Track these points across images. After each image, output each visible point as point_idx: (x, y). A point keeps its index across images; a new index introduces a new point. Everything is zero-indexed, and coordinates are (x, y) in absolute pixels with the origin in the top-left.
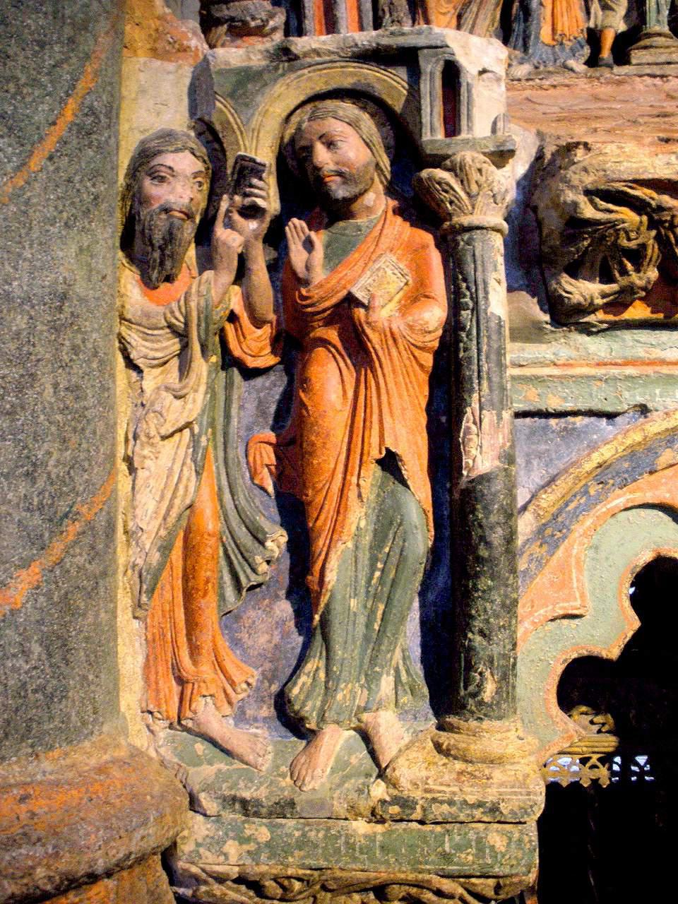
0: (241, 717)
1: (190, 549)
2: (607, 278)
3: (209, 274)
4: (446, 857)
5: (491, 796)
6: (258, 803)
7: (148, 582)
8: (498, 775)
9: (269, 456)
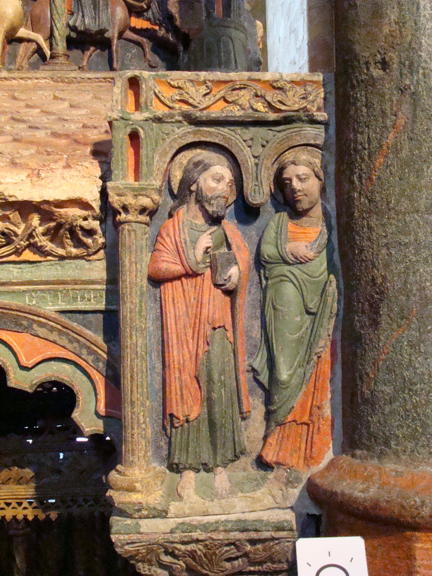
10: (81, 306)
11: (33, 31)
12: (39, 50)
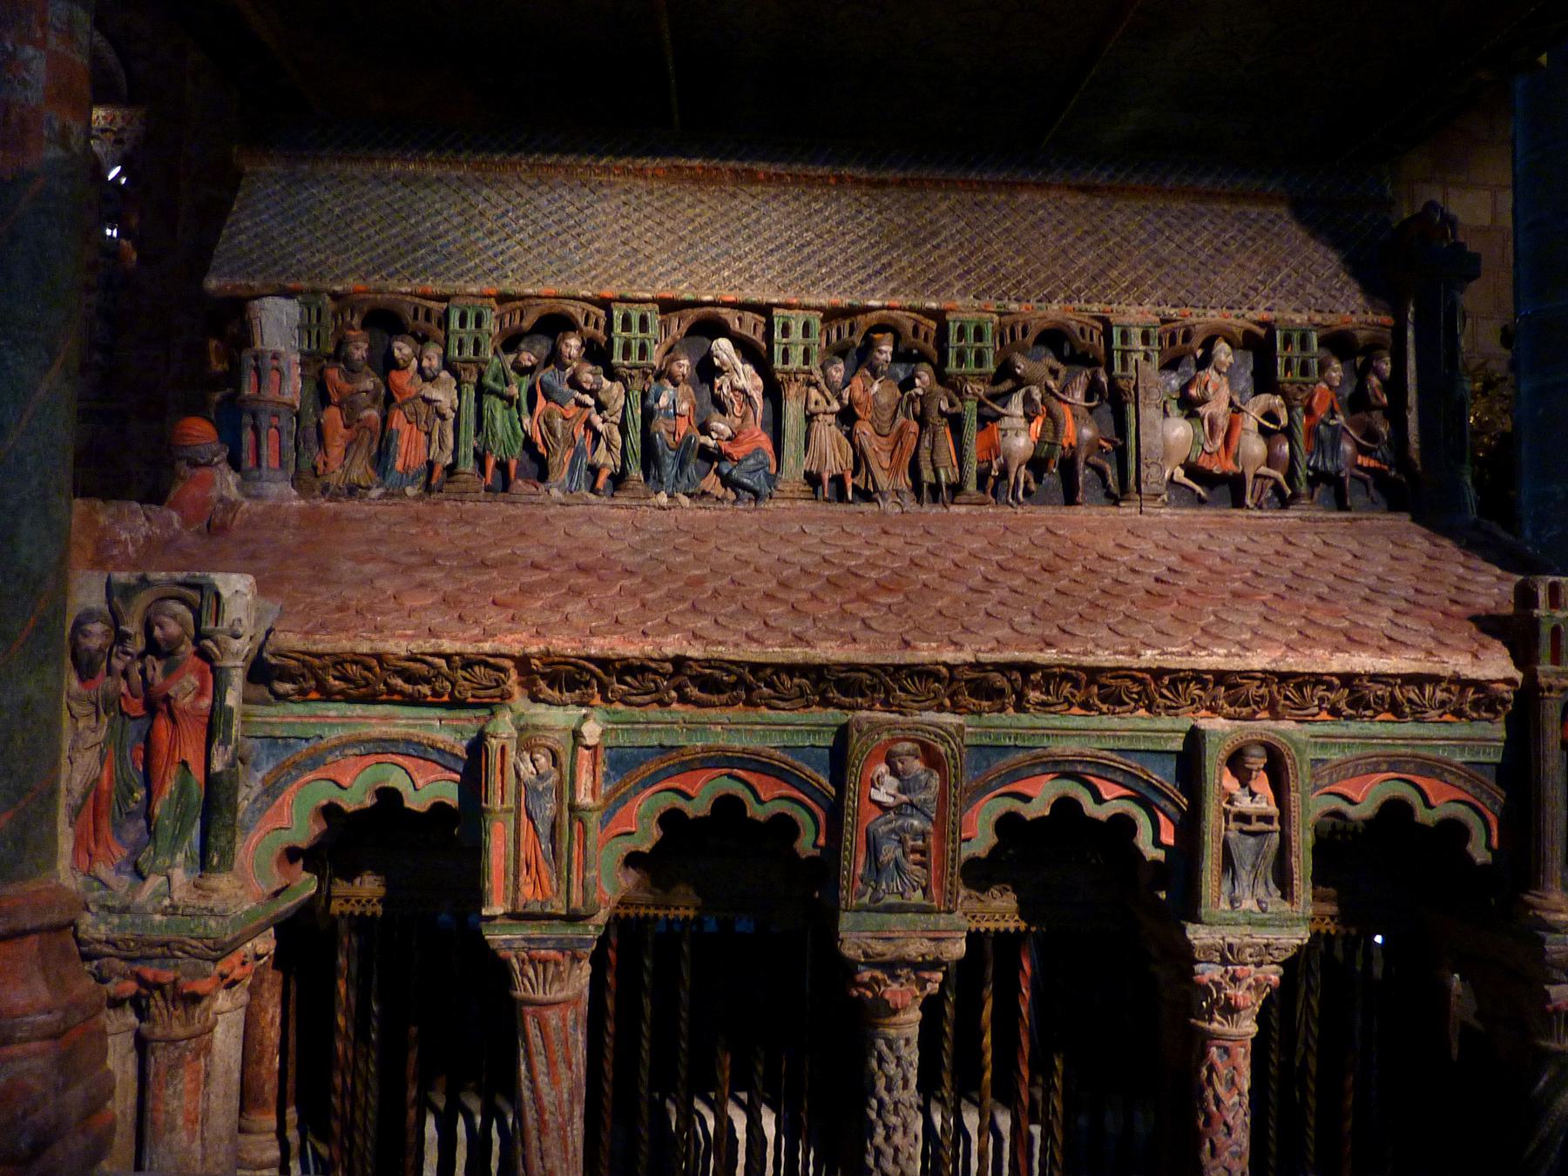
0: (118, 871)
1: (96, 798)
2: (294, 683)
3: (109, 679)
4: (192, 931)
5: (211, 904)
6: (114, 907)
7: (76, 812)
8: (215, 896)
9: (141, 754)
10: (1482, 759)
11: (1268, 466)
12: (1277, 488)
